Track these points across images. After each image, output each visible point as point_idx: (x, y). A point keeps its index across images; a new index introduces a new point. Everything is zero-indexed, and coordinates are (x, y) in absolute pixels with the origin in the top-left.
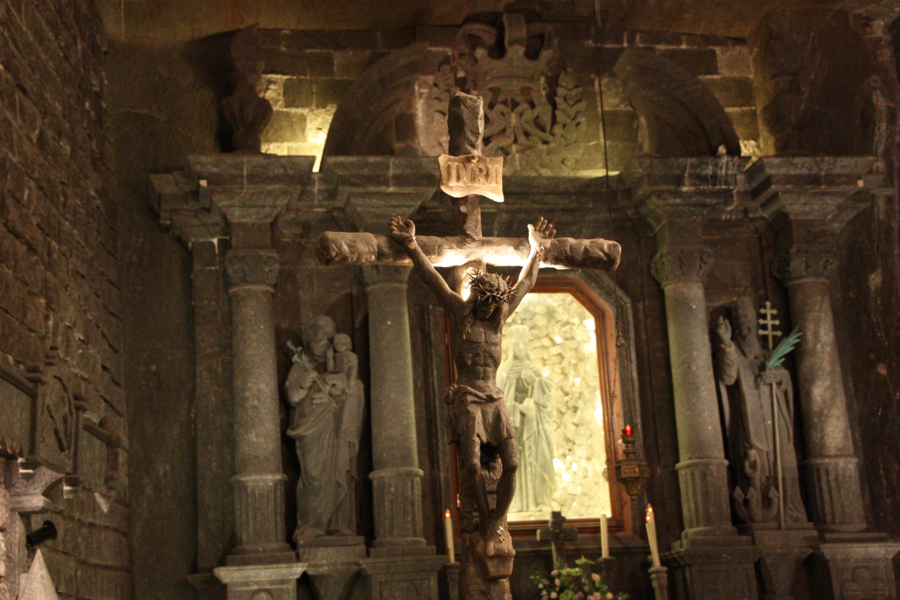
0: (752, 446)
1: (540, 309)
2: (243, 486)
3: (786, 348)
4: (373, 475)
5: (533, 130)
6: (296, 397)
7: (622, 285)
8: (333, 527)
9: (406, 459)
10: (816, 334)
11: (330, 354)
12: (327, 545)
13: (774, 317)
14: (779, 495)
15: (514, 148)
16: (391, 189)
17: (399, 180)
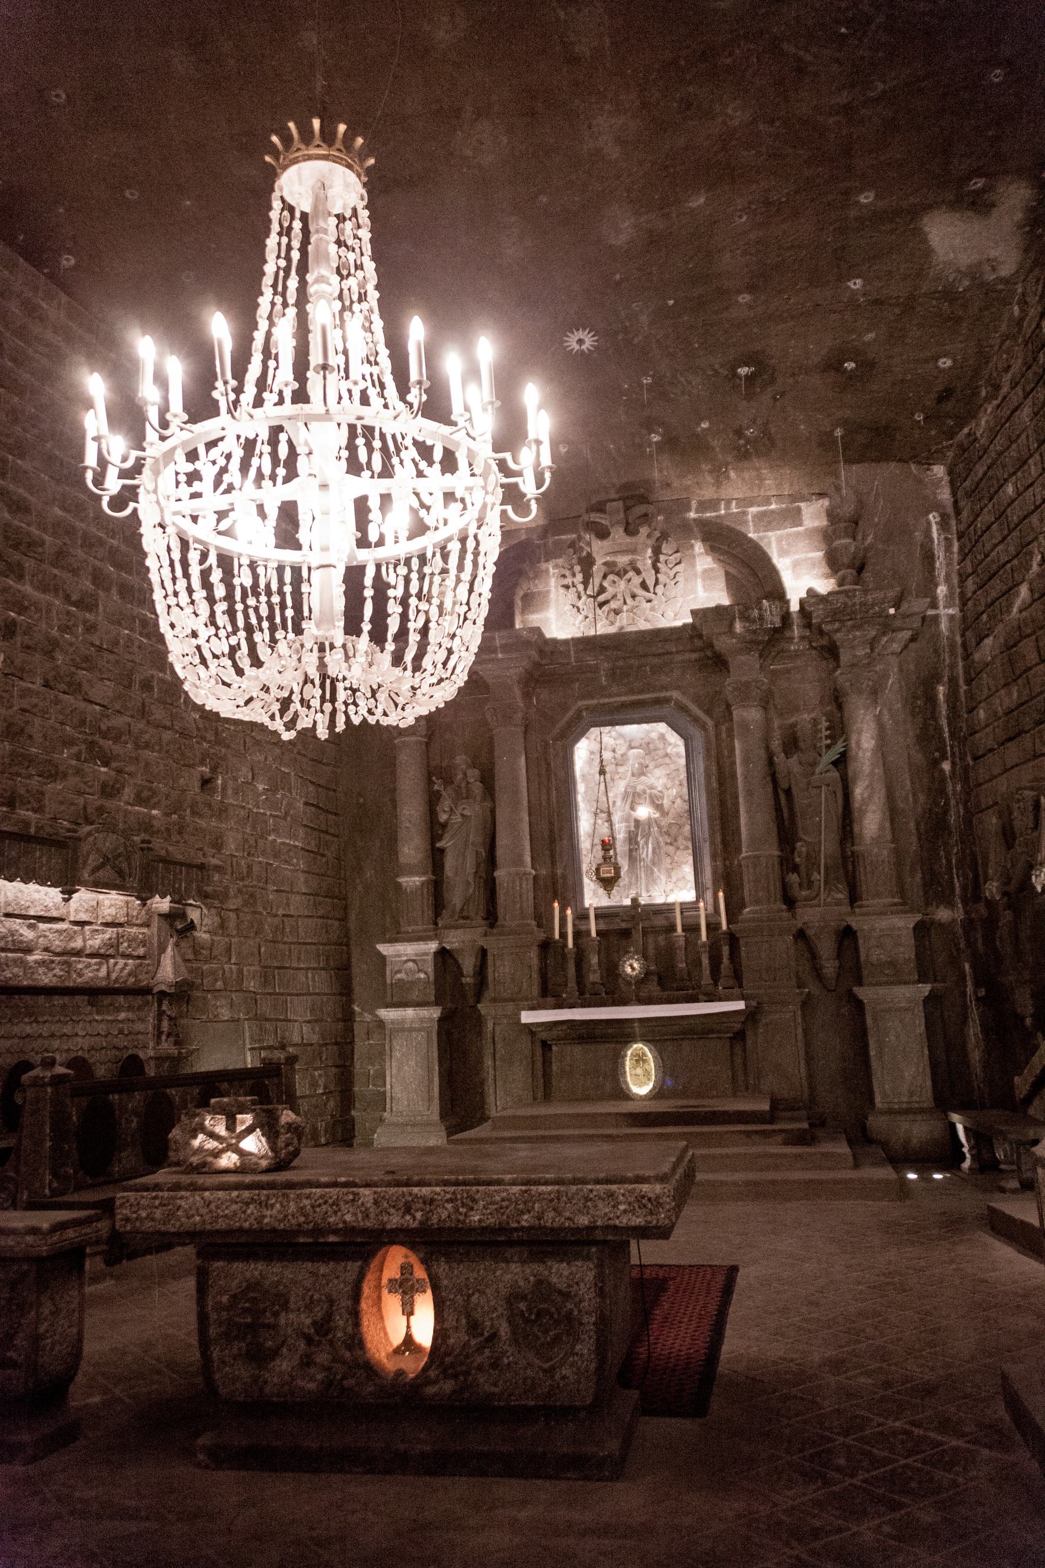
0: (801, 840)
1: (654, 735)
2: (398, 886)
3: (833, 755)
4: (497, 874)
5: (640, 592)
6: (443, 817)
7: (708, 712)
8: (465, 914)
9: (519, 861)
10: (858, 743)
11: (463, 785)
12: (456, 927)
13: (827, 729)
14: (818, 877)
15: (625, 608)
16: (500, 656)
17: (505, 648)
